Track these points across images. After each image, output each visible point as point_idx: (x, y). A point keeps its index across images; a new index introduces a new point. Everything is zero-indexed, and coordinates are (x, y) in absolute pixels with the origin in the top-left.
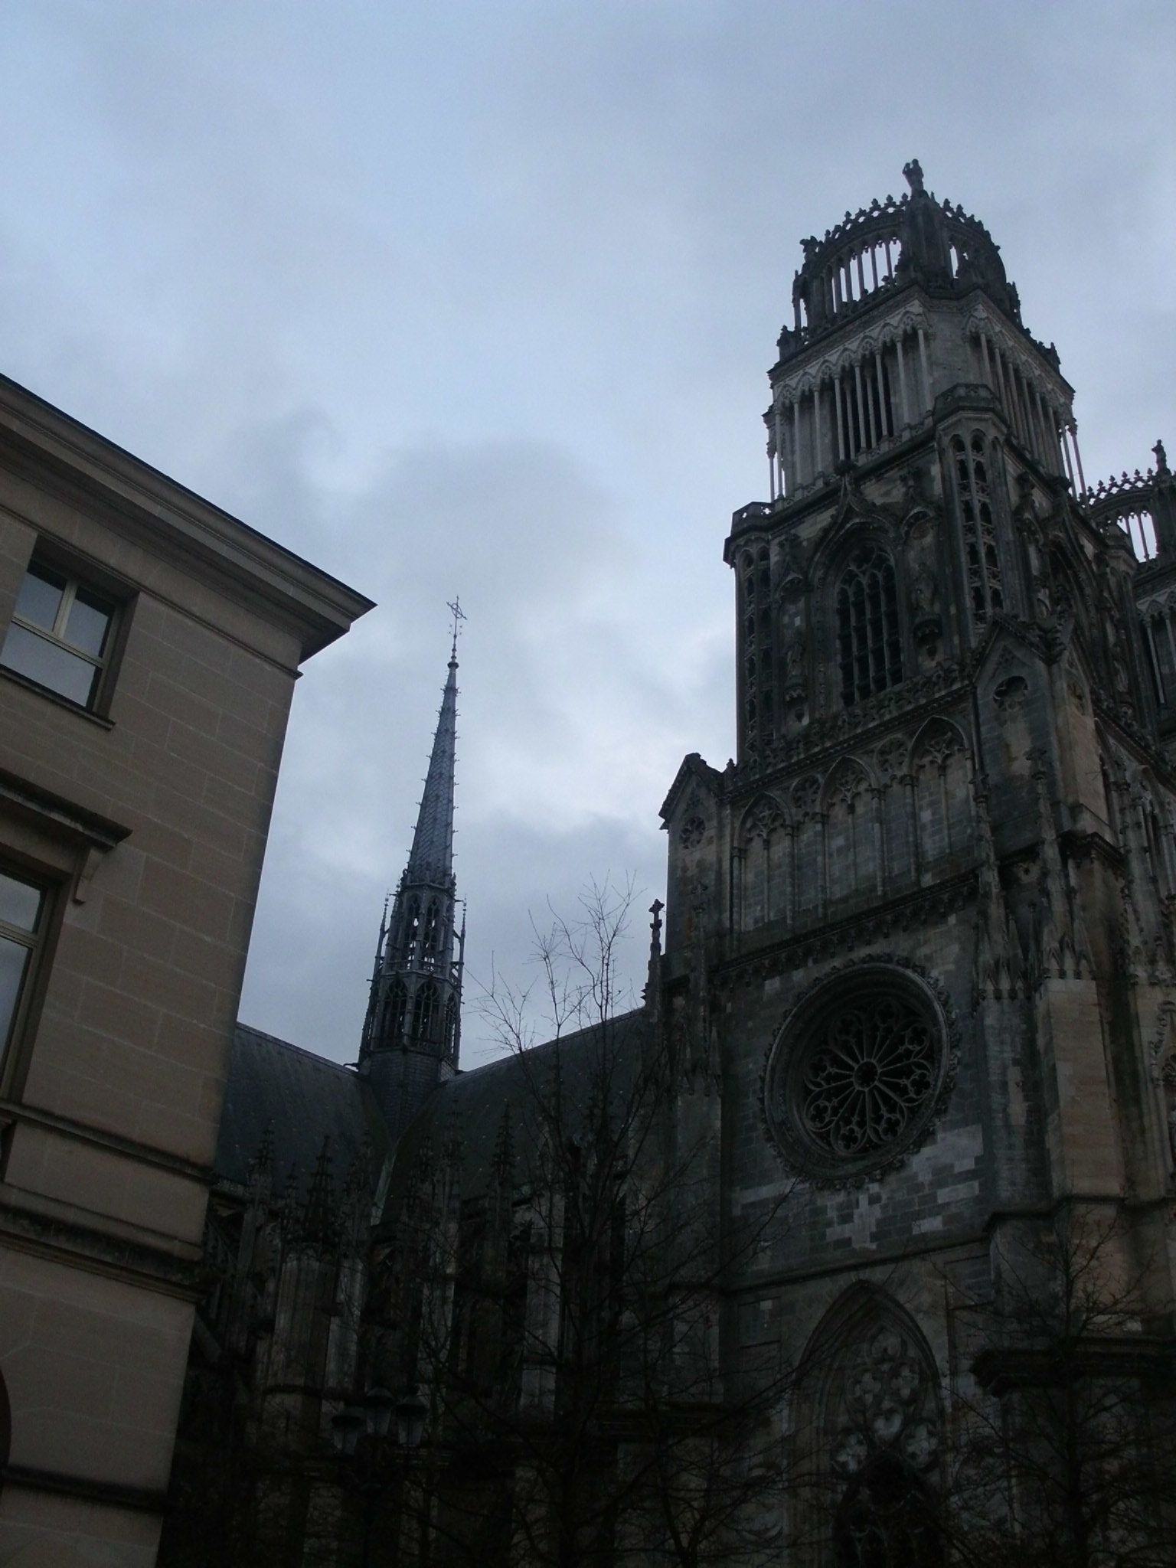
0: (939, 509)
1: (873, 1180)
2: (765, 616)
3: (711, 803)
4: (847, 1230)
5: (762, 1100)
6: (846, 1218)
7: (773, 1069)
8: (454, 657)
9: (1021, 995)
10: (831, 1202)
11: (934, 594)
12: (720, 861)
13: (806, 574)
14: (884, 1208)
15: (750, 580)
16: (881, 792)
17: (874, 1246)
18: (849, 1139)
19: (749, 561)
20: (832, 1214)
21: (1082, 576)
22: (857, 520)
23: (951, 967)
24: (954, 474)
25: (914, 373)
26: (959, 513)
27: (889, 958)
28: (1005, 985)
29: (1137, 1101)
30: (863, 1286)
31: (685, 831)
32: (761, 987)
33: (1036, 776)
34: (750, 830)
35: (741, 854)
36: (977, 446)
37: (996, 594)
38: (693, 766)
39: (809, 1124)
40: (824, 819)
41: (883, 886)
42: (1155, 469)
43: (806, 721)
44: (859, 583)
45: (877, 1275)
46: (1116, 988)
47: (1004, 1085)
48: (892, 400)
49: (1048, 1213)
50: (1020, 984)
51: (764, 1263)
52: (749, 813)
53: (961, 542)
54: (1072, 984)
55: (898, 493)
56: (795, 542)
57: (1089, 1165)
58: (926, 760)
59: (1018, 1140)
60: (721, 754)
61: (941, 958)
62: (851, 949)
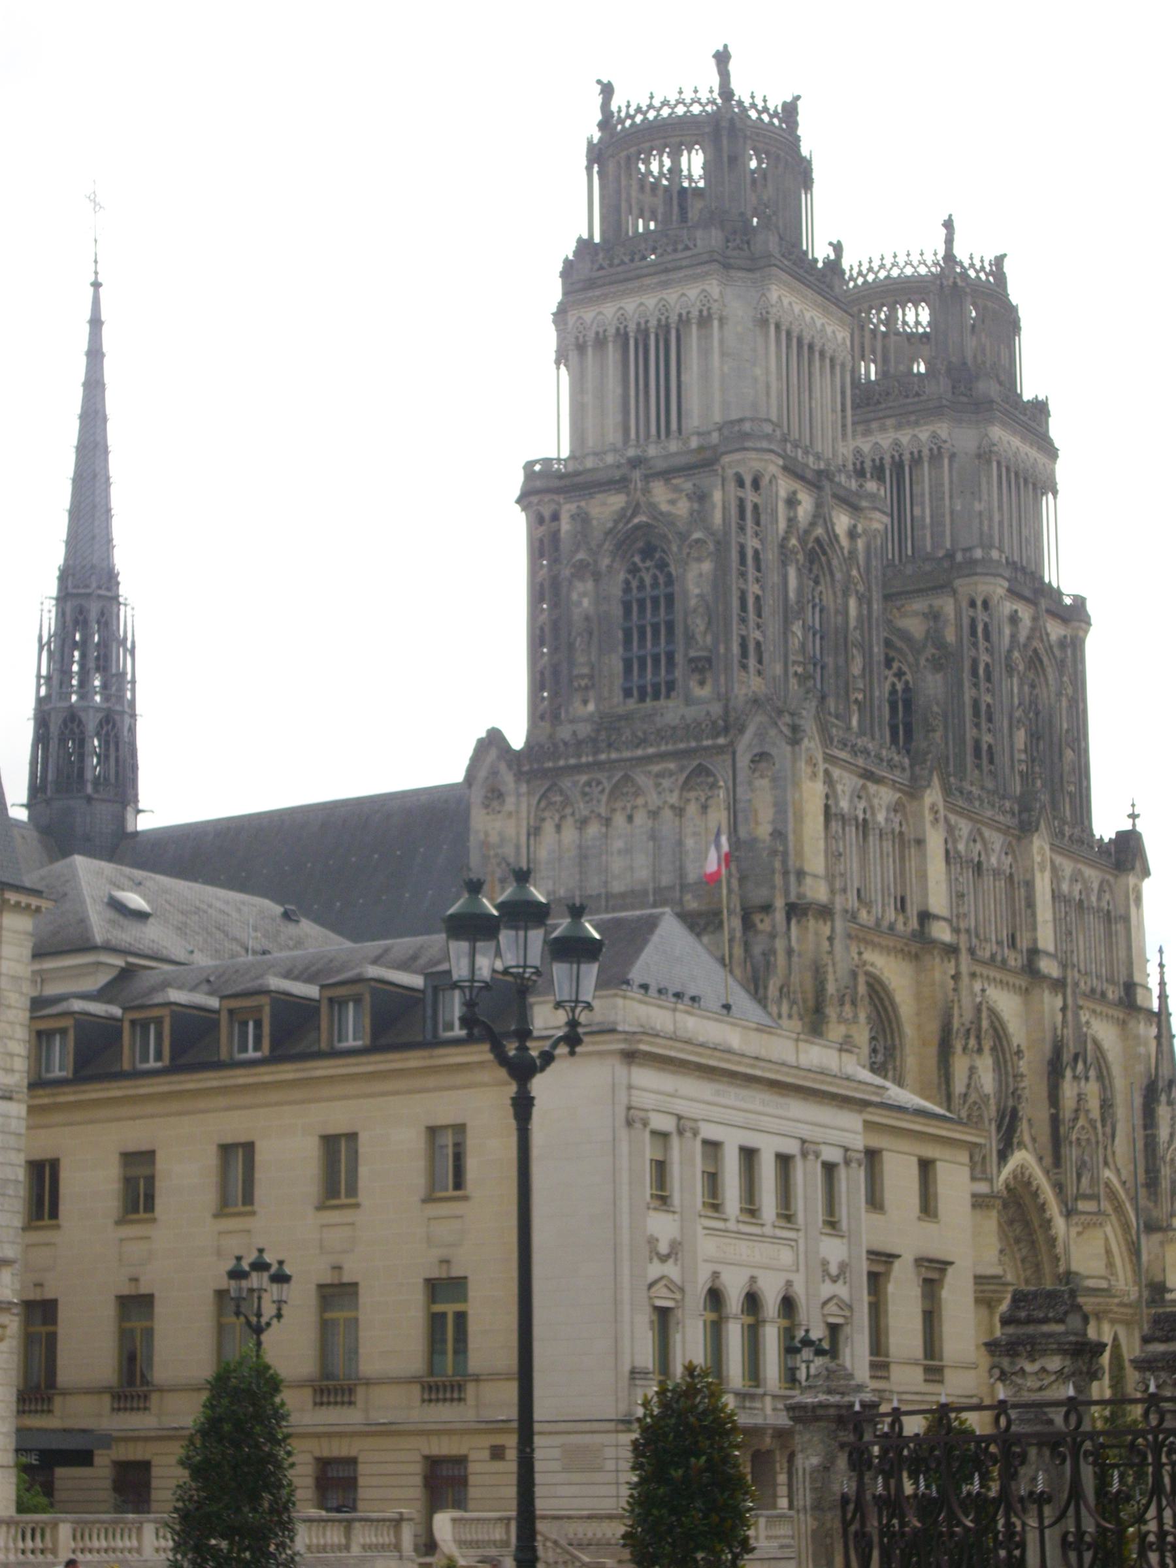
0: (718, 543)
2: (555, 582)
8: (96, 273)
11: (707, 629)
12: (518, 834)
15: (541, 541)
16: (654, 814)
19: (541, 520)
21: (835, 562)
22: (644, 519)
25: (705, 353)
31: (486, 797)
33: (774, 853)
34: (544, 810)
35: (535, 832)
36: (756, 485)
37: (758, 644)
38: (493, 741)
40: (608, 822)
41: (654, 894)
42: (941, 253)
44: (642, 581)
48: (683, 378)
52: (544, 796)
53: (734, 587)
55: (683, 508)
56: (582, 518)
58: (692, 795)
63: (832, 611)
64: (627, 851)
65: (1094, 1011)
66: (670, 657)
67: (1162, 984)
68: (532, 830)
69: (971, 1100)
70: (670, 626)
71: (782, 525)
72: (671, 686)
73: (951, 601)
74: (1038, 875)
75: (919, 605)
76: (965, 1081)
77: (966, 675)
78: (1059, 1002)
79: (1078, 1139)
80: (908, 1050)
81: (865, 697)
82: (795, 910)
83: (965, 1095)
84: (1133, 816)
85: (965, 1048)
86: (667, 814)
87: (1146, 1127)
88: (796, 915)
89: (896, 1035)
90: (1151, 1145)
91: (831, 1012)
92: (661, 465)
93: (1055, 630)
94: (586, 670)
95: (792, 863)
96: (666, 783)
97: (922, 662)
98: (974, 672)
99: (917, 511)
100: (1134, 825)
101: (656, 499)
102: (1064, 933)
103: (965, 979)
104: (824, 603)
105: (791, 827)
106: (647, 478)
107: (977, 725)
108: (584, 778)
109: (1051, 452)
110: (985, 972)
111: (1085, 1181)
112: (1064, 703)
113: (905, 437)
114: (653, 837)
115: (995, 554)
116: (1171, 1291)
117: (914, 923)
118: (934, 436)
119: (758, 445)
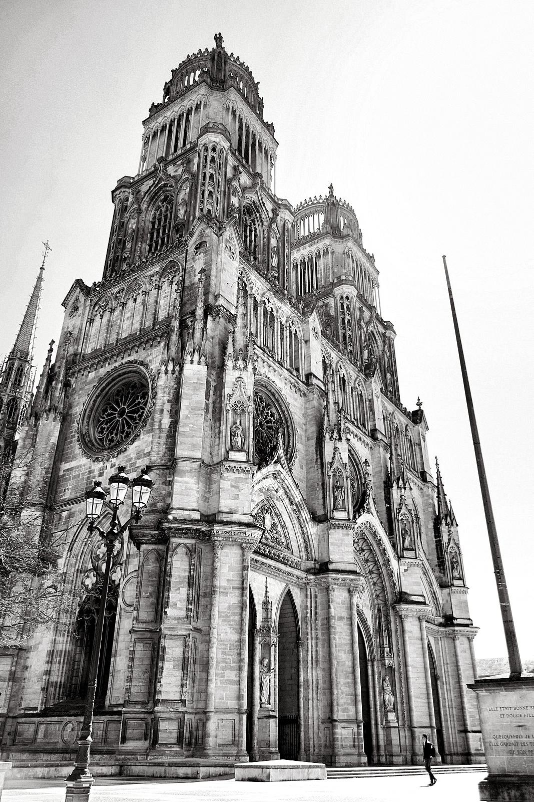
1: (113, 457)
3: (82, 298)
5: (78, 424)
7: (85, 410)
9: (177, 373)
10: (97, 467)
12: (82, 324)
16: (146, 293)
20: (96, 473)
21: (263, 216)
22: (163, 183)
26: (200, 177)
27: (136, 362)
28: (170, 368)
29: (220, 420)
32: (87, 376)
35: (91, 321)
36: (214, 150)
40: (124, 305)
42: (328, 195)
44: (161, 210)
46: (218, 369)
47: (162, 411)
50: (177, 368)
51: (67, 495)
53: (199, 190)
59: (164, 435)
67: (438, 472)
68: (89, 320)
69: (335, 466)
73: (333, 299)
76: (332, 455)
79: (402, 519)
83: (332, 463)
85: (331, 437)
86: (154, 292)
87: (436, 537)
88: (211, 314)
89: (290, 428)
90: (439, 544)
91: (230, 363)
95: (213, 289)
96: (154, 279)
98: (343, 323)
99: (319, 276)
104: (258, 233)
114: (144, 304)
116: (457, 619)
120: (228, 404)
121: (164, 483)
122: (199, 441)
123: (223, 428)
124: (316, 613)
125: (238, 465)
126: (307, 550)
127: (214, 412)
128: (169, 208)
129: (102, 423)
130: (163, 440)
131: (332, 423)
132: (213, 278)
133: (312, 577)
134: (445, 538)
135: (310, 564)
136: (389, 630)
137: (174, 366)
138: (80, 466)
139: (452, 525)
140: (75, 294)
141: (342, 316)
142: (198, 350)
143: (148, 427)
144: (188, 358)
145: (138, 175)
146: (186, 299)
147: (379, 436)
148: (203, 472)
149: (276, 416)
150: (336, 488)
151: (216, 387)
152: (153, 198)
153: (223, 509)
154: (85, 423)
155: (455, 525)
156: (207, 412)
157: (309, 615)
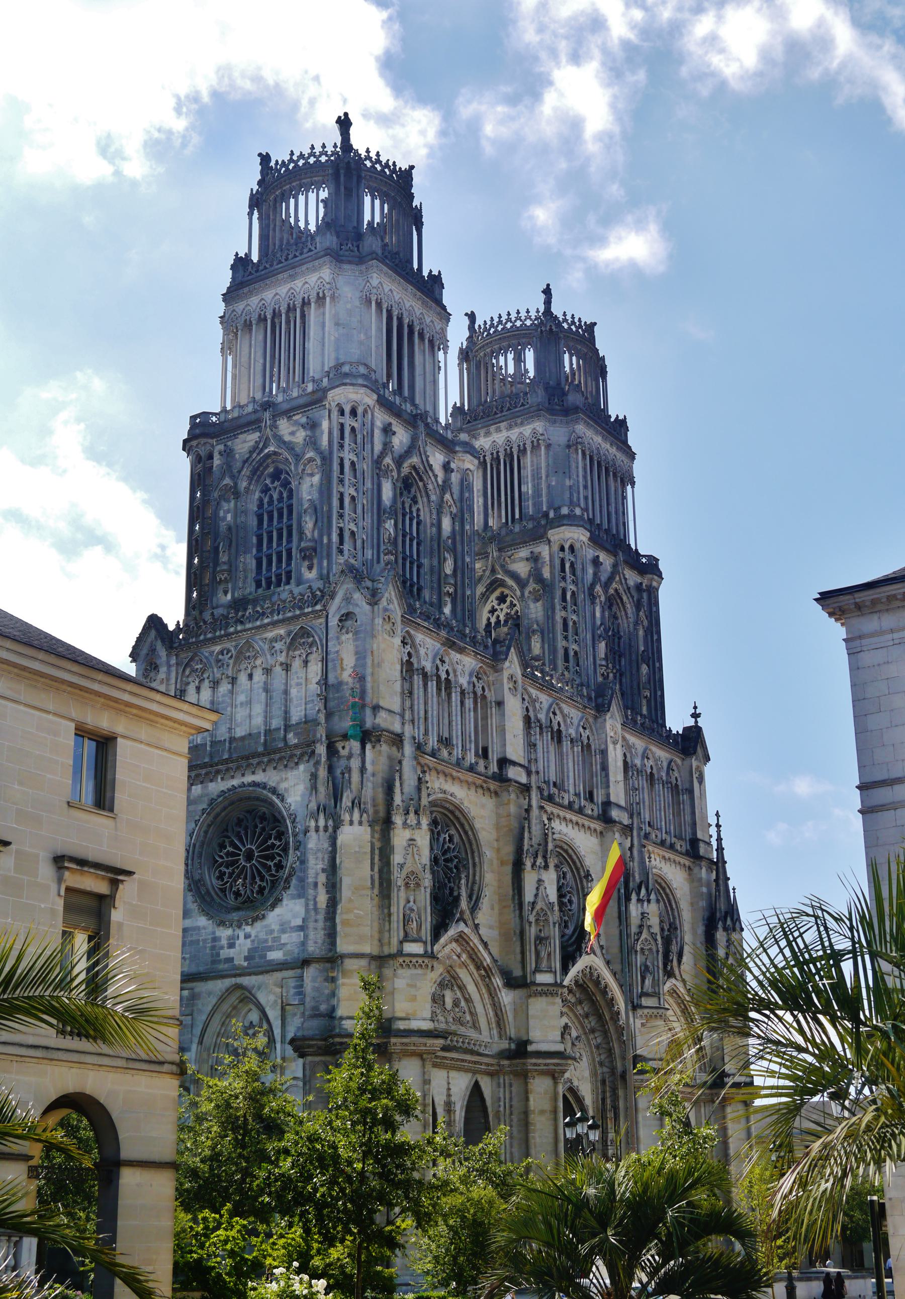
0: (323, 459)
1: (247, 924)
3: (162, 652)
4: (231, 953)
6: (231, 945)
7: (194, 845)
9: (330, 829)
10: (224, 933)
13: (236, 484)
14: (253, 941)
16: (268, 671)
17: (246, 964)
18: (237, 894)
20: (224, 942)
21: (430, 486)
22: (272, 449)
23: (299, 799)
24: (336, 433)
26: (336, 467)
27: (264, 786)
28: (322, 823)
30: (239, 987)
31: (146, 670)
36: (354, 412)
38: (154, 623)
39: (214, 881)
40: (233, 681)
42: (542, 310)
43: (229, 597)
44: (271, 497)
45: (246, 981)
49: (332, 960)
50: (330, 823)
53: (335, 491)
54: (356, 828)
55: (300, 436)
56: (228, 453)
57: (358, 933)
58: (297, 653)
59: (321, 917)
60: (174, 615)
61: (294, 788)
62: (243, 775)
63: (428, 525)
64: (249, 702)
65: (664, 857)
66: (289, 552)
67: (719, 840)
69: (538, 907)
70: (290, 528)
71: (378, 447)
72: (289, 574)
73: (547, 547)
74: (611, 747)
75: (524, 553)
76: (534, 892)
77: (557, 601)
78: (628, 844)
79: (642, 949)
80: (486, 867)
81: (456, 590)
82: (366, 736)
83: (534, 903)
84: (695, 716)
85: (534, 865)
86: (278, 669)
89: (476, 854)
91: (398, 820)
92: (285, 406)
93: (632, 577)
94: (225, 567)
96: (278, 646)
97: (526, 594)
98: (564, 599)
99: (524, 489)
100: (696, 722)
101: (281, 433)
102: (631, 790)
103: (535, 812)
104: (422, 518)
105: (369, 670)
106: (274, 417)
107: (566, 638)
108: (218, 648)
109: (632, 456)
110: (562, 814)
111: (648, 982)
112: (641, 633)
113: (514, 434)
114: (266, 690)
115: (578, 511)
117: (494, 768)
118: (534, 432)
119: (354, 382)
120: (398, 877)
121: (326, 980)
122: (366, 930)
123: (394, 909)
124: (511, 1106)
125: (414, 960)
126: (498, 1024)
127: (381, 884)
128: (285, 495)
129: (221, 865)
130: (321, 924)
131: (535, 841)
132: (369, 679)
133: (506, 1062)
134: (721, 952)
135: (505, 1045)
136: (615, 1109)
137: (326, 822)
138: (198, 928)
139: (734, 930)
140: (149, 640)
141: (563, 584)
142: (357, 803)
143: (292, 891)
144: (346, 817)
145: (224, 410)
146: (331, 704)
147: (615, 814)
148: (373, 967)
149: (456, 839)
150: (540, 940)
151: (383, 852)
152: (256, 474)
153: (399, 1014)
154: (197, 865)
155: (738, 929)
156: (373, 888)
157: (502, 1109)
